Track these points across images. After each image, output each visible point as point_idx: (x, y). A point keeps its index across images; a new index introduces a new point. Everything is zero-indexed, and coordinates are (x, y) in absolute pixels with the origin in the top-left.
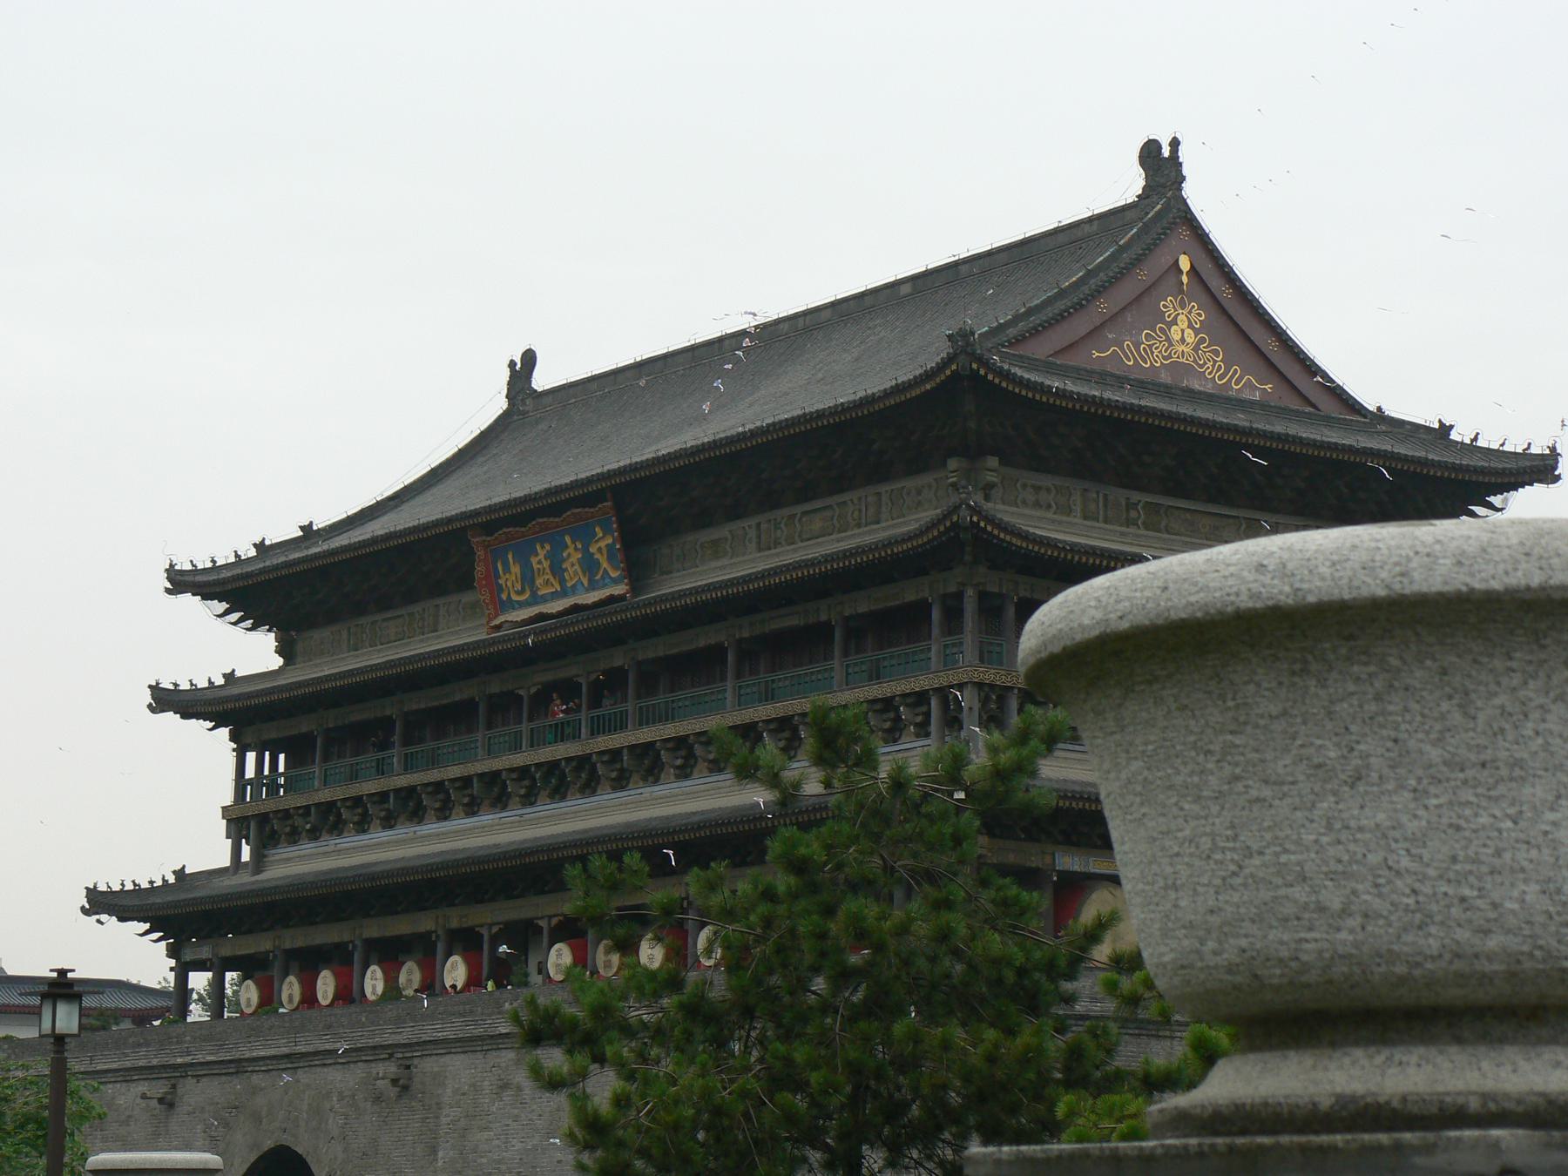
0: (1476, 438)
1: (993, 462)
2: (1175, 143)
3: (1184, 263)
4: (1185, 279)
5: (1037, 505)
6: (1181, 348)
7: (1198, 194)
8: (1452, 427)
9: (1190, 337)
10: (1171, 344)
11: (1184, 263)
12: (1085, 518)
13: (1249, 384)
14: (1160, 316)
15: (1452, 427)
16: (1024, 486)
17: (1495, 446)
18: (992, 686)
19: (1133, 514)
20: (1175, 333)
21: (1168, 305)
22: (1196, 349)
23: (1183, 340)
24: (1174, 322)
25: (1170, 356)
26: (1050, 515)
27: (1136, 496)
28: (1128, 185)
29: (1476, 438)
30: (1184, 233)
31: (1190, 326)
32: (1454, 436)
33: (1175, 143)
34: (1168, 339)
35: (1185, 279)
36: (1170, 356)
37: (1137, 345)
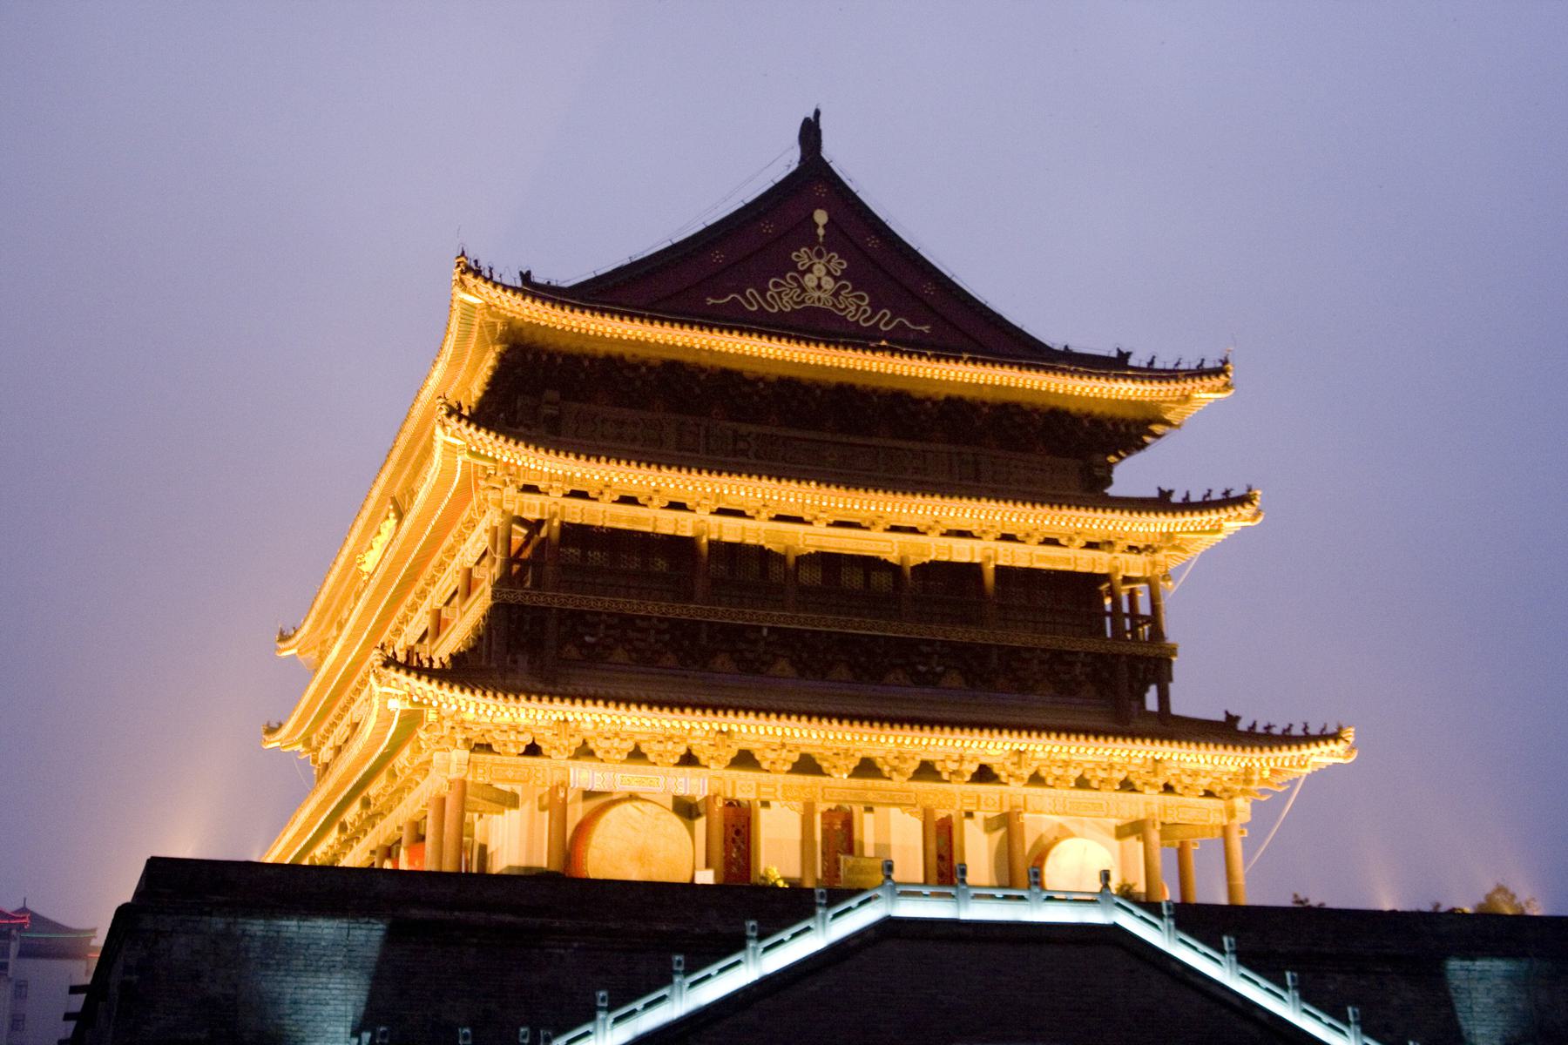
0: (1152, 363)
1: (552, 395)
2: (817, 113)
3: (821, 217)
4: (821, 232)
5: (620, 437)
6: (817, 294)
7: (833, 151)
8: (1129, 354)
9: (828, 284)
10: (804, 290)
11: (821, 217)
12: (680, 450)
13: (901, 326)
14: (793, 266)
15: (1129, 354)
16: (604, 421)
17: (1170, 366)
18: (521, 607)
19: (742, 445)
20: (810, 281)
21: (802, 257)
22: (836, 294)
23: (819, 287)
24: (810, 270)
25: (803, 301)
26: (637, 447)
27: (744, 429)
28: (785, 160)
29: (1152, 363)
30: (821, 191)
31: (829, 273)
32: (1132, 362)
33: (817, 113)
34: (800, 286)
35: (821, 232)
36: (803, 301)
37: (763, 293)
